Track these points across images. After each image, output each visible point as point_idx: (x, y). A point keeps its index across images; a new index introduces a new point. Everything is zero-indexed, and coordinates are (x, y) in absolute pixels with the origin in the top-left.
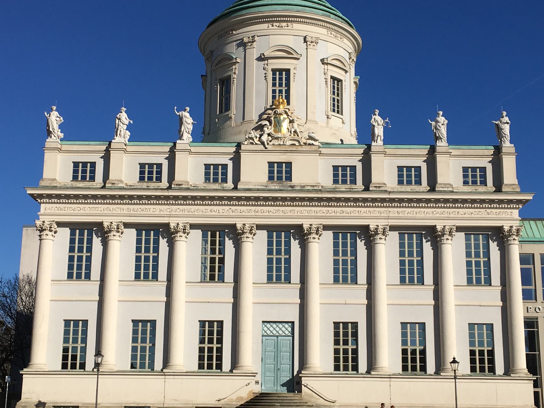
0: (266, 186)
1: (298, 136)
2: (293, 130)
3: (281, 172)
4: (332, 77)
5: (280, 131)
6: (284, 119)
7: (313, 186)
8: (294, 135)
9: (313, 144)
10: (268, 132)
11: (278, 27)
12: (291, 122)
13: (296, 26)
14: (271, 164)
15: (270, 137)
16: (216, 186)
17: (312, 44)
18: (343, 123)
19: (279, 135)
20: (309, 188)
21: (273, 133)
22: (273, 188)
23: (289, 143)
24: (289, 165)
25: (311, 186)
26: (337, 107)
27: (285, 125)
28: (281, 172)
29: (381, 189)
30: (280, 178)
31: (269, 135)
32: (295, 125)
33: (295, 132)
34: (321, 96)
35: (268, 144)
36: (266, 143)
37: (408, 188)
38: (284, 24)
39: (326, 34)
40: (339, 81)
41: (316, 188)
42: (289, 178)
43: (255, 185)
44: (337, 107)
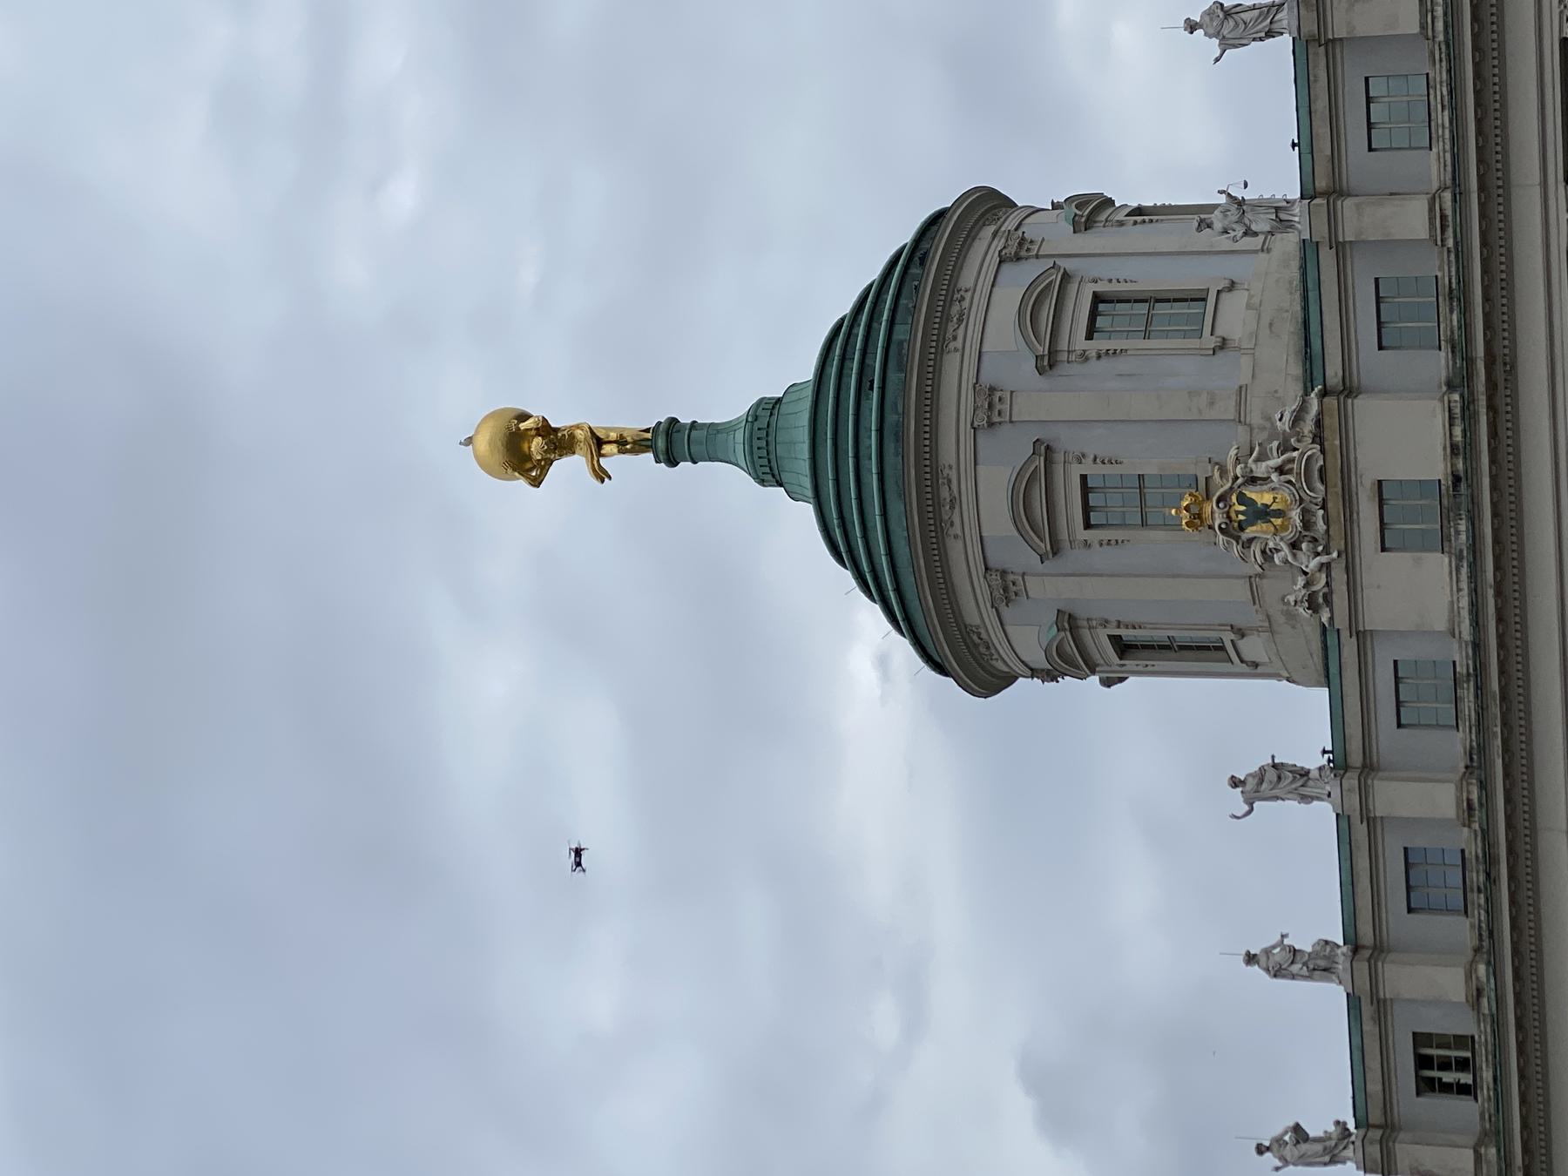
0: (1460, 558)
1: (1292, 460)
2: (1274, 477)
4: (1089, 337)
5: (1280, 513)
6: (1242, 499)
7: (1451, 418)
8: (1290, 472)
9: (1321, 413)
10: (1286, 550)
11: (952, 508)
12: (1253, 480)
13: (947, 454)
15: (1304, 546)
17: (998, 407)
18: (1232, 286)
19: (1295, 515)
20: (1458, 431)
21: (1289, 535)
22: (1463, 537)
25: (1451, 425)
27: (1263, 497)
29: (1449, 212)
31: (1294, 546)
32: (1260, 470)
33: (1281, 470)
35: (1327, 551)
36: (1324, 559)
38: (945, 493)
39: (958, 355)
40: (1098, 299)
41: (1458, 411)
43: (1459, 590)
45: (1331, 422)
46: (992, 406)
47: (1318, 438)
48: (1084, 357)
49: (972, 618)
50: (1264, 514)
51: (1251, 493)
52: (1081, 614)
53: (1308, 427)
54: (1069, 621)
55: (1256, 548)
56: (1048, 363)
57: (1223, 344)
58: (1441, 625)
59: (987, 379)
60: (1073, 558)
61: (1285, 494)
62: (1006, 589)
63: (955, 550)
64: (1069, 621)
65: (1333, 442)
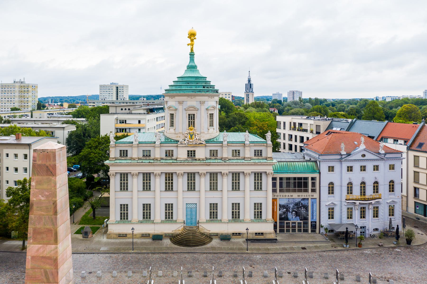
3: (191, 154)
13: (197, 98)
14: (188, 151)
16: (169, 158)
19: (191, 141)
23: (194, 143)
24: (194, 151)
26: (211, 125)
27: (193, 136)
28: (191, 154)
30: (191, 156)
32: (196, 137)
34: (206, 121)
37: (236, 158)
42: (194, 156)
44: (211, 125)
45: (202, 145)
46: (202, 103)
47: (200, 143)
48: (207, 113)
49: (176, 98)
50: (191, 136)
51: (194, 135)
52: (177, 111)
53: (201, 142)
54: (176, 110)
55: (187, 135)
56: (207, 109)
57: (208, 130)
58: (179, 157)
59: (206, 102)
60: (184, 112)
61: (194, 140)
62: (180, 103)
63: (186, 98)
64: (176, 110)
65: (200, 145)
